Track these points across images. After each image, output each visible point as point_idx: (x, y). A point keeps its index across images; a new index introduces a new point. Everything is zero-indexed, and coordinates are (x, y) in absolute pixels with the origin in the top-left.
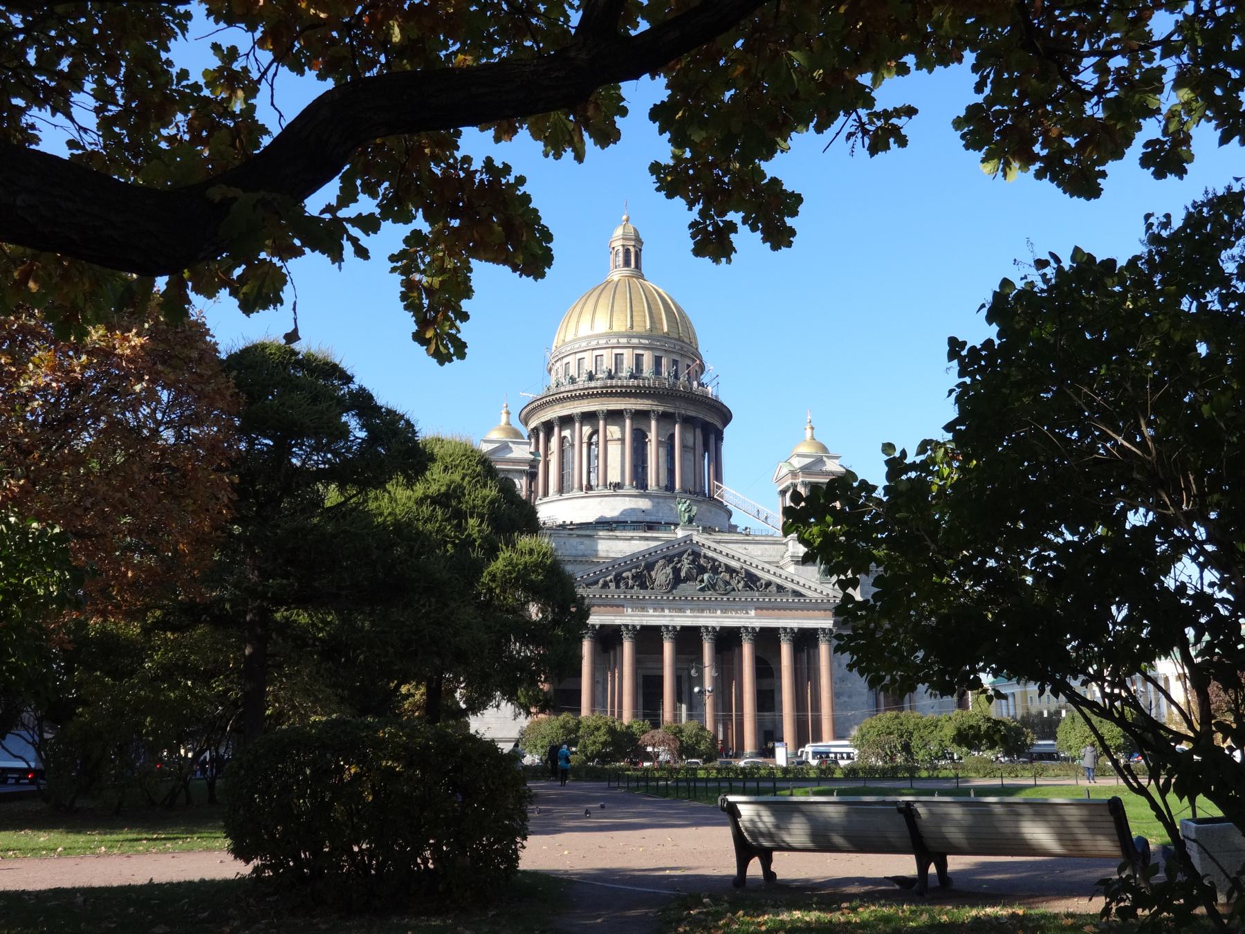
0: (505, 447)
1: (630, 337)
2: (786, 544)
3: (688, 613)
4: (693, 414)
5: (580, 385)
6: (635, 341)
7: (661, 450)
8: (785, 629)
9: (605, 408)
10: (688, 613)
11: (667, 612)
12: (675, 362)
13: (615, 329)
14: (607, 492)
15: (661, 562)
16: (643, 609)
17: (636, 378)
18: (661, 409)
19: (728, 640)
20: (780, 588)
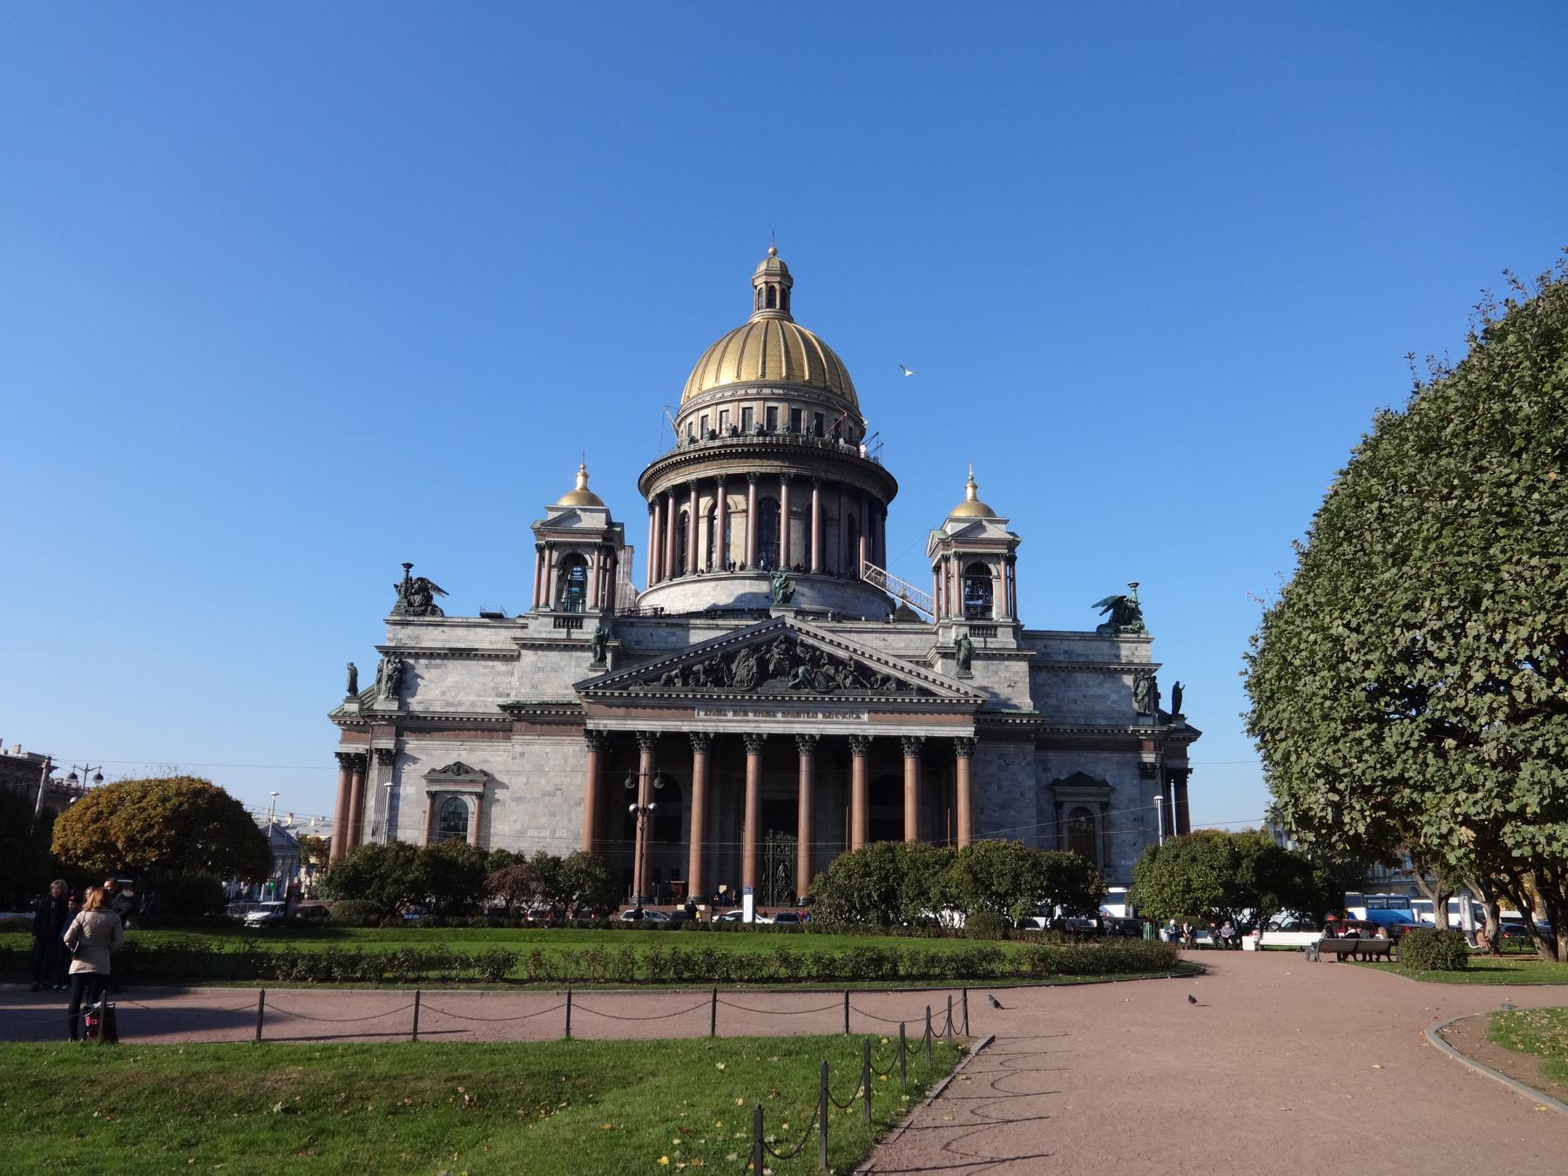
0: (571, 515)
1: (761, 386)
2: (936, 633)
3: (779, 716)
4: (837, 477)
5: (702, 444)
6: (767, 391)
7: (795, 523)
8: (908, 738)
9: (723, 472)
10: (779, 716)
11: (751, 716)
12: (819, 417)
13: (744, 378)
14: (724, 574)
15: (743, 652)
16: (720, 712)
17: (765, 435)
18: (793, 471)
19: (832, 752)
20: (902, 685)
